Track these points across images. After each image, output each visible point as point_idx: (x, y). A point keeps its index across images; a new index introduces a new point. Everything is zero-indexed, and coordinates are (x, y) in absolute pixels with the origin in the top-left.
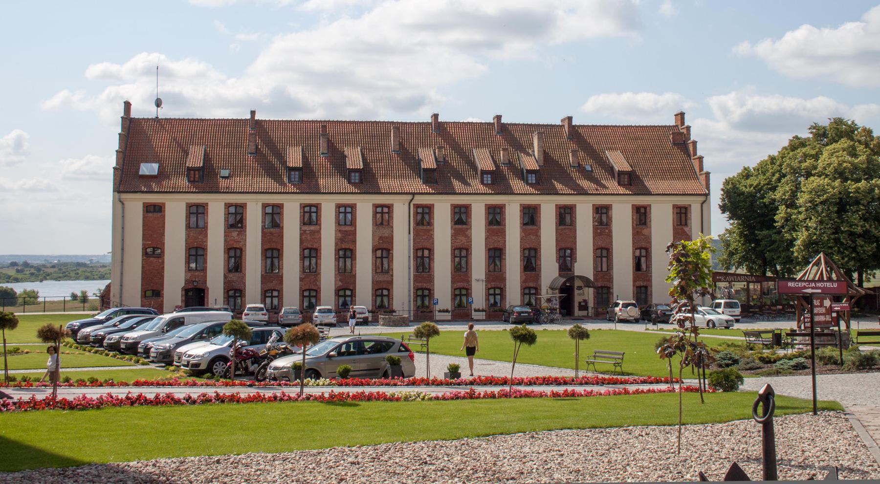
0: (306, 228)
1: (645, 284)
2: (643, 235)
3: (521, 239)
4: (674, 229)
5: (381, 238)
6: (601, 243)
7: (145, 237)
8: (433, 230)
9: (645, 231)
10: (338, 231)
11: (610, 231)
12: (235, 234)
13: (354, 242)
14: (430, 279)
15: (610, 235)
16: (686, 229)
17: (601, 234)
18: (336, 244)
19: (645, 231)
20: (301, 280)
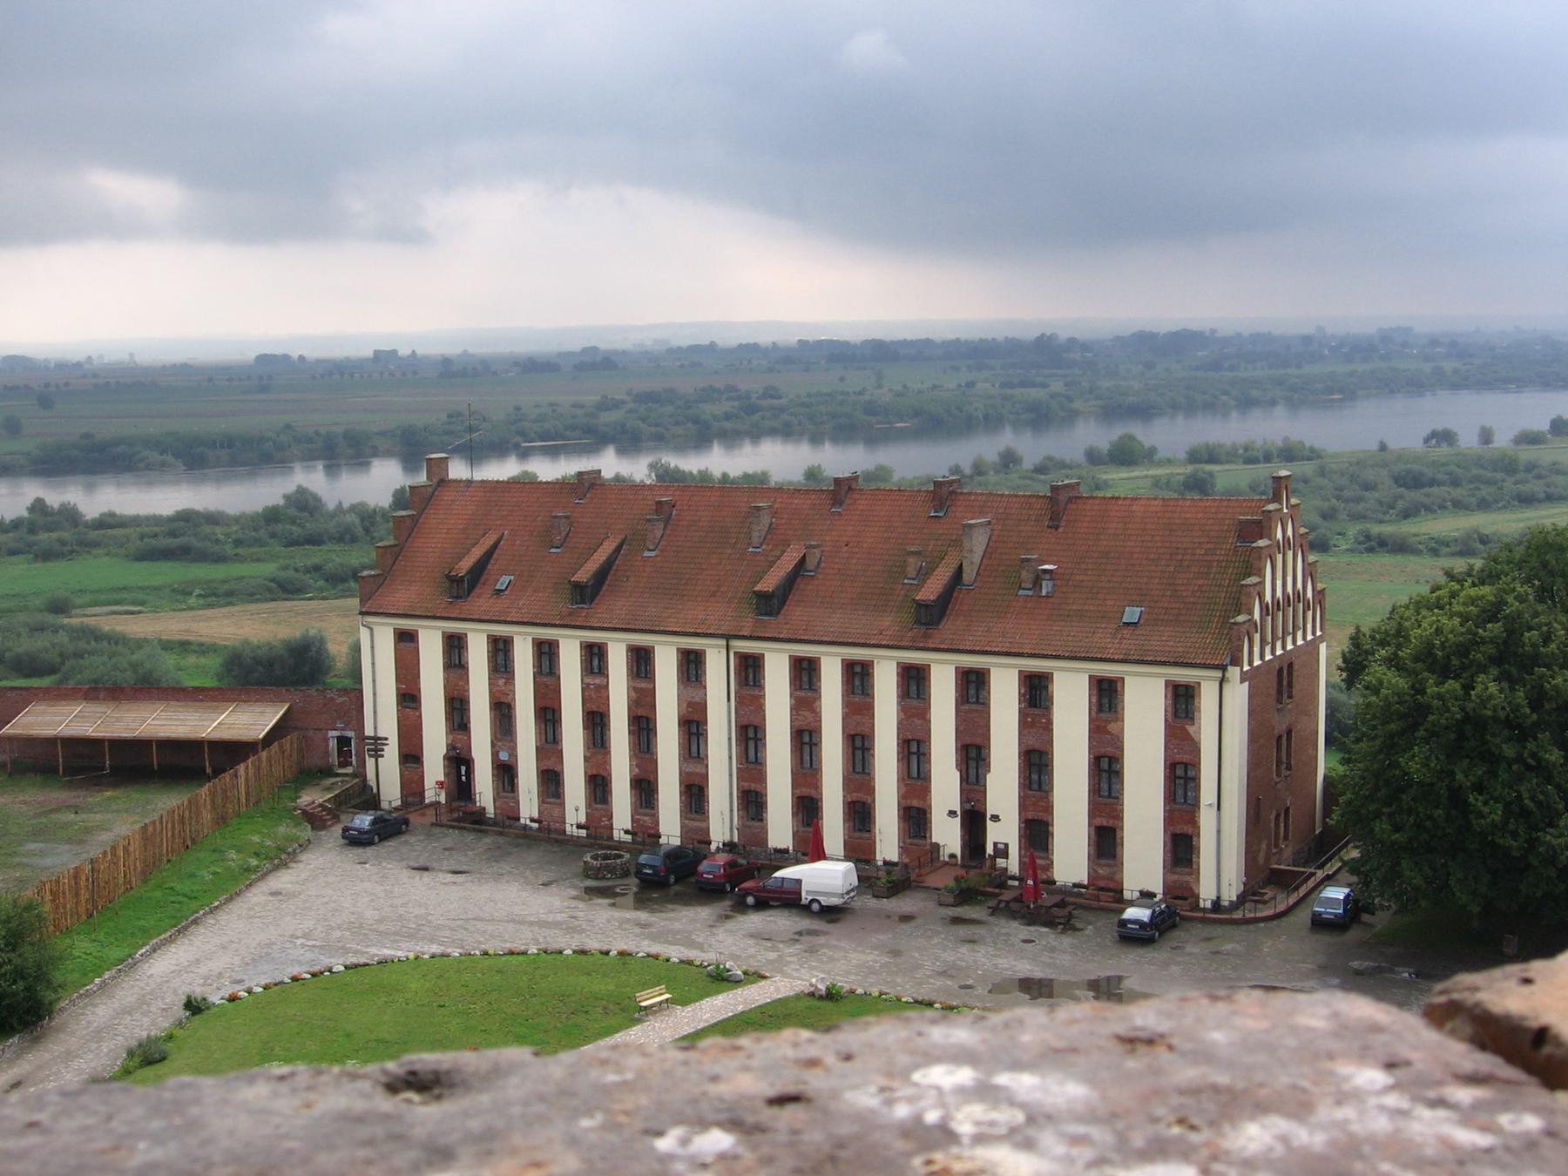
0: (588, 680)
1: (1111, 823)
2: (1109, 733)
3: (900, 723)
4: (1168, 726)
5: (690, 704)
6: (1033, 742)
7: (399, 679)
8: (763, 696)
9: (1112, 727)
10: (632, 689)
11: (1050, 722)
12: (501, 682)
13: (654, 707)
14: (761, 777)
15: (1048, 728)
16: (1191, 729)
17: (1032, 725)
18: (629, 708)
19: (1112, 727)
20: (586, 759)
